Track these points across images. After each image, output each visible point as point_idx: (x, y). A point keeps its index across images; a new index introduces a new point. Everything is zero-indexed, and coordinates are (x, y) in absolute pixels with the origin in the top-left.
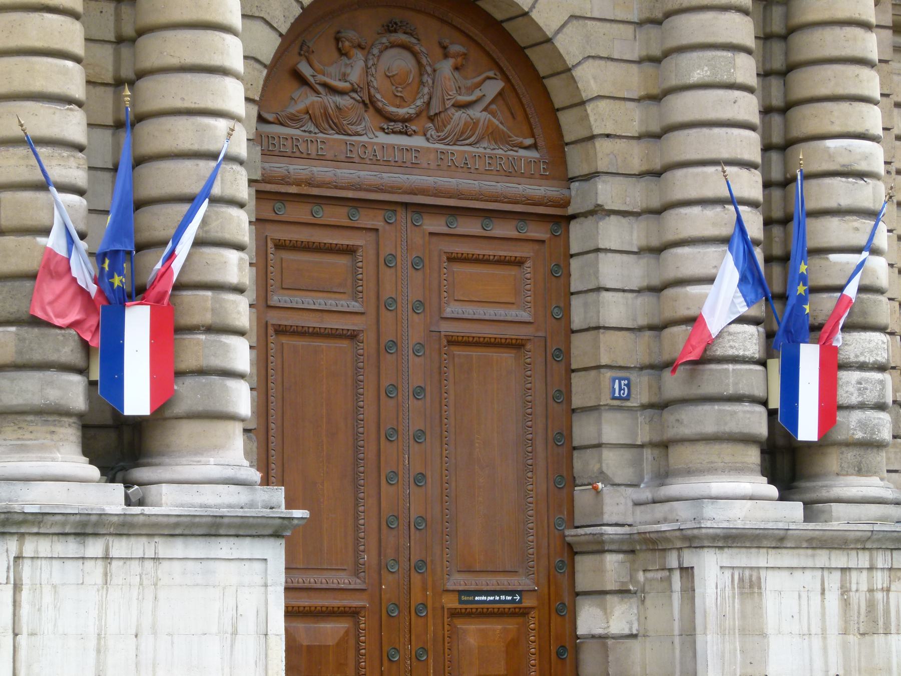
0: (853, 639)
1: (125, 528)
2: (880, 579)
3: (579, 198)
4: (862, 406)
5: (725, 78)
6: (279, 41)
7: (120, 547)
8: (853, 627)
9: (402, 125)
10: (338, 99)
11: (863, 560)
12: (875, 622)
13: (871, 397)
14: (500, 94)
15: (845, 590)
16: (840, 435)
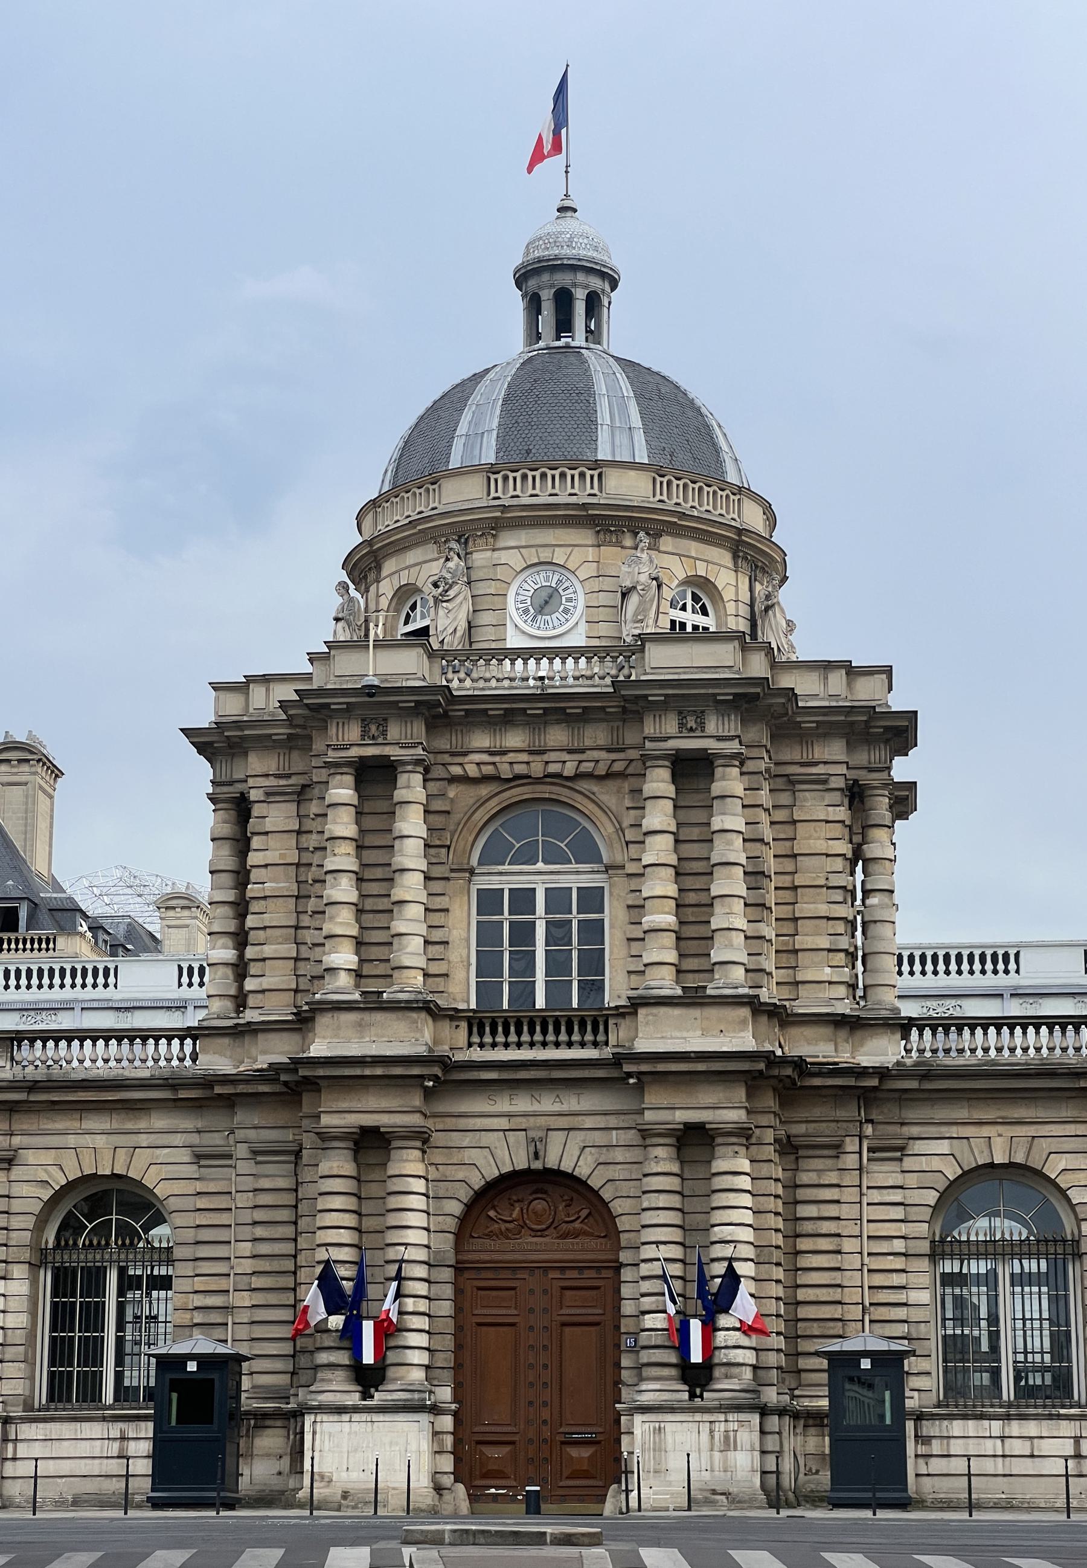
0: (717, 1455)
1: (355, 1409)
2: (732, 1426)
3: (624, 1257)
4: (726, 1347)
5: (653, 1205)
6: (463, 1206)
7: (356, 1417)
8: (716, 1448)
9: (541, 1233)
10: (508, 1225)
11: (722, 1417)
12: (729, 1445)
13: (730, 1343)
14: (589, 1214)
15: (711, 1431)
16: (716, 1361)
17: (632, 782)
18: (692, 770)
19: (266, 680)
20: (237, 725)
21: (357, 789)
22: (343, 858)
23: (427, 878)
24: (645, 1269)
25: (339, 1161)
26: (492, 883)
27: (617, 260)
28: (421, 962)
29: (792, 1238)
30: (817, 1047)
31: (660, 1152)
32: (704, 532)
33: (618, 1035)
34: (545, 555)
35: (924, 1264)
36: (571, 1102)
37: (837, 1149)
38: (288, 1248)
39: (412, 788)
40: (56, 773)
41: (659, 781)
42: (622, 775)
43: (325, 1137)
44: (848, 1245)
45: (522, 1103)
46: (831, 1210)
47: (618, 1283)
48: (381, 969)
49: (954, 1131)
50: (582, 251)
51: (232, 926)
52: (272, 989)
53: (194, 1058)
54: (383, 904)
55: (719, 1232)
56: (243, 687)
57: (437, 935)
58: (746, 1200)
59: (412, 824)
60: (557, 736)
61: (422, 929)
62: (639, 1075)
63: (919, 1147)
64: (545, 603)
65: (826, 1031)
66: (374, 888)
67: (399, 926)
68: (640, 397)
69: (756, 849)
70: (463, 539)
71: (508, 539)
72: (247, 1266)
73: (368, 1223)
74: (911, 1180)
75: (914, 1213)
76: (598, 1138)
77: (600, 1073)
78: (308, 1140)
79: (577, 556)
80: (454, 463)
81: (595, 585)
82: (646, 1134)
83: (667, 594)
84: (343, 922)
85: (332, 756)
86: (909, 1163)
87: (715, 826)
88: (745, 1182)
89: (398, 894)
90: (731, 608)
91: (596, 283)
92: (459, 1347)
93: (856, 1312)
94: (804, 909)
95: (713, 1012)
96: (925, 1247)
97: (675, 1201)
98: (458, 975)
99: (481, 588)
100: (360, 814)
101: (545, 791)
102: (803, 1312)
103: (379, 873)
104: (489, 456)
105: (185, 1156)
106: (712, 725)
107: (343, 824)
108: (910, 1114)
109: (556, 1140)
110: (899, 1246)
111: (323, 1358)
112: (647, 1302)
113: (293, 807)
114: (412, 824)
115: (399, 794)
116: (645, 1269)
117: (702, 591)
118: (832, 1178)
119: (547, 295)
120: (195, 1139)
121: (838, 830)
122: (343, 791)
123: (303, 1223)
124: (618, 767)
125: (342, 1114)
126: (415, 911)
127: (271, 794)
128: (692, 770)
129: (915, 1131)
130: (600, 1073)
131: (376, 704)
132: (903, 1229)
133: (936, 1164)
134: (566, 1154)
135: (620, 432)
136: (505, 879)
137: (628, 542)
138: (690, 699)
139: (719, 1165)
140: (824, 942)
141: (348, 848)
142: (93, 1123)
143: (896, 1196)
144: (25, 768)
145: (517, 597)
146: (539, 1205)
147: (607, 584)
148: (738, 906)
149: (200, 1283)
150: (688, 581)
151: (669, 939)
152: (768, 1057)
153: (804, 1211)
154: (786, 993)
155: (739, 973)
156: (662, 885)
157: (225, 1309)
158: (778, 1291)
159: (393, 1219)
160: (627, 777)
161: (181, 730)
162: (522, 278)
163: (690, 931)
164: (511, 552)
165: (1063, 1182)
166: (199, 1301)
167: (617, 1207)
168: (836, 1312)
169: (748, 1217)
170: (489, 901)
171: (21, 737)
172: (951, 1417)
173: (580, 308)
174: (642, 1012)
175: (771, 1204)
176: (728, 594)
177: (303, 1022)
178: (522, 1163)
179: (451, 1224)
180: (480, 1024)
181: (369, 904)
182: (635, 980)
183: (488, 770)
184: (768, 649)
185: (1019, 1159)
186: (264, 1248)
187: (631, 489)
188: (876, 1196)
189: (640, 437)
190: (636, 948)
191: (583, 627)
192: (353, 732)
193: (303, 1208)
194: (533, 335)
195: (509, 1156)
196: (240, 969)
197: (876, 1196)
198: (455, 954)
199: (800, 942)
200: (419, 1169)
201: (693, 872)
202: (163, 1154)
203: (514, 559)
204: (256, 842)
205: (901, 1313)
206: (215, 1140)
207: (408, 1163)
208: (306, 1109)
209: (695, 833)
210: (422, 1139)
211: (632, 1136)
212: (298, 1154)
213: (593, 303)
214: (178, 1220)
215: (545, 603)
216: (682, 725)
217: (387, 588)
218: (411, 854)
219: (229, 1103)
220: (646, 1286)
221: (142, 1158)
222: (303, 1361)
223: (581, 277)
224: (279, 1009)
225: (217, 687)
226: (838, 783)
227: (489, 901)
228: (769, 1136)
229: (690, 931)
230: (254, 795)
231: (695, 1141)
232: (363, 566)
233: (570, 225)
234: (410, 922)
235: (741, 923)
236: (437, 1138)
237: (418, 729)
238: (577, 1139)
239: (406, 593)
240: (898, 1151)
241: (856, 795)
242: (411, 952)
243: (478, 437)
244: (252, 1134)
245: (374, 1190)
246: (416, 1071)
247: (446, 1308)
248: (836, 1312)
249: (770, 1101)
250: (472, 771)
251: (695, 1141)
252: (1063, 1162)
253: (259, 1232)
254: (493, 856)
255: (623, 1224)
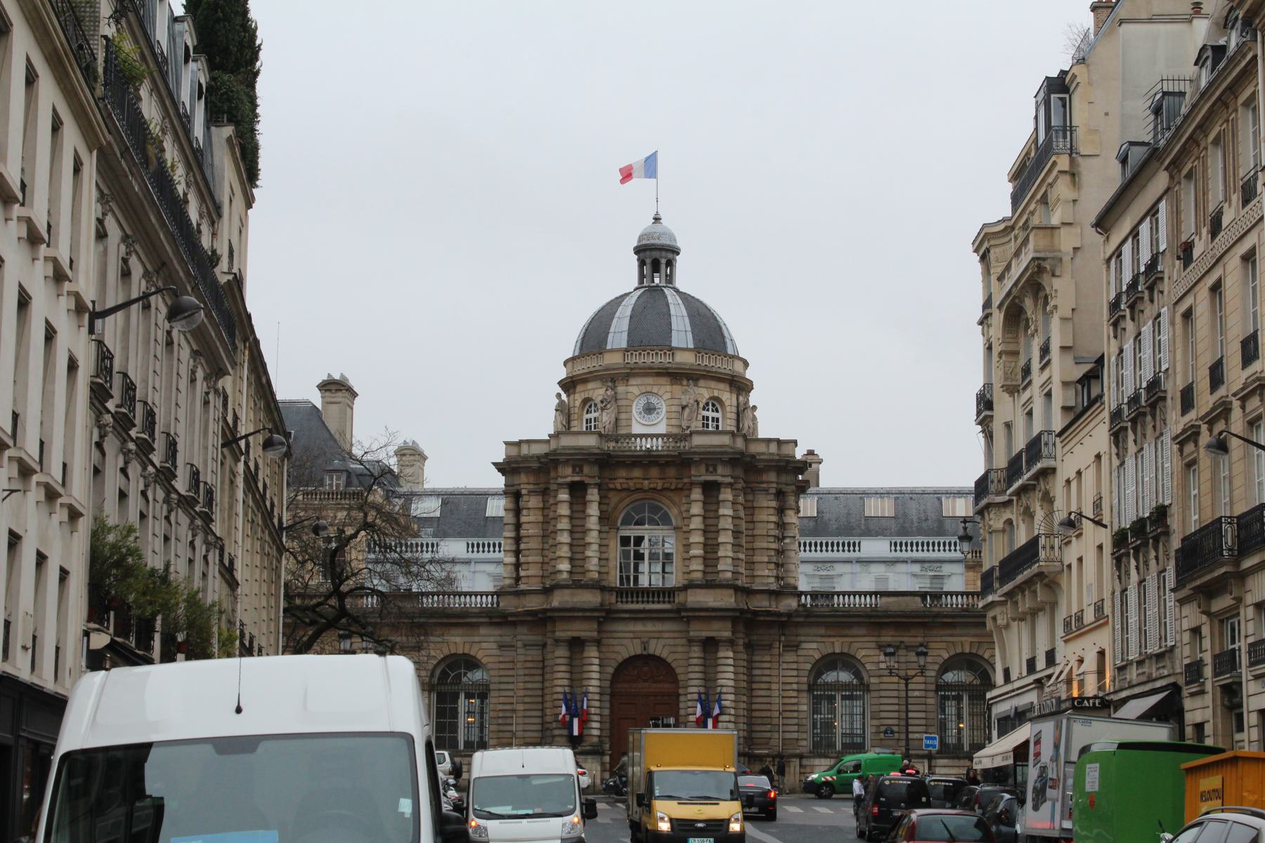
3: (681, 691)
17: (686, 492)
18: (710, 489)
19: (528, 442)
20: (517, 462)
21: (571, 494)
22: (564, 524)
23: (600, 532)
24: (689, 697)
25: (562, 652)
26: (626, 533)
27: (679, 244)
28: (597, 568)
29: (749, 686)
30: (761, 603)
31: (696, 649)
32: (718, 378)
33: (679, 598)
34: (649, 389)
35: (805, 695)
36: (659, 627)
37: (770, 646)
38: (540, 685)
39: (593, 495)
40: (354, 395)
41: (697, 494)
42: (681, 489)
43: (557, 641)
44: (774, 686)
45: (639, 627)
46: (767, 672)
47: (678, 702)
48: (580, 570)
49: (819, 639)
50: (664, 241)
51: (514, 548)
52: (532, 575)
53: (498, 604)
54: (581, 542)
55: (721, 682)
56: (519, 443)
57: (604, 556)
58: (731, 669)
59: (593, 510)
60: (654, 472)
61: (598, 554)
62: (688, 617)
63: (804, 645)
64: (649, 409)
65: (765, 596)
66: (577, 536)
67: (589, 553)
68: (690, 316)
69: (737, 522)
70: (613, 381)
71: (633, 381)
72: (521, 693)
73: (576, 676)
74: (801, 659)
75: (801, 673)
76: (671, 642)
77: (671, 615)
78: (549, 642)
79: (663, 389)
80: (609, 347)
81: (670, 402)
82: (691, 641)
83: (701, 405)
84: (564, 551)
85: (560, 480)
86: (800, 652)
87: (720, 526)
88: (731, 661)
89: (588, 539)
90: (728, 409)
91: (670, 256)
92: (611, 728)
93: (776, 714)
94: (758, 545)
95: (718, 591)
96: (805, 687)
97: (701, 669)
98: (612, 572)
99: (621, 403)
100: (571, 504)
101: (649, 495)
102: (755, 714)
103: (579, 529)
104: (624, 345)
105: (494, 646)
106: (720, 470)
107: (564, 510)
108: (802, 631)
109: (653, 642)
110: (795, 686)
111: (557, 732)
112: (690, 710)
113: (540, 498)
114: (593, 510)
115: (589, 497)
116: (689, 697)
117: (716, 403)
118: (768, 658)
119: (648, 261)
120: (499, 639)
121: (772, 511)
122: (564, 496)
123: (547, 676)
124: (680, 486)
125: (566, 631)
126: (595, 547)
127: (530, 492)
128: (710, 489)
129: (803, 638)
130: (671, 615)
131: (579, 459)
132: (796, 680)
133: (811, 652)
134: (656, 648)
135: (682, 333)
136: (632, 532)
137: (685, 382)
138: (711, 459)
139: (721, 654)
140: (766, 559)
141: (566, 520)
142: (454, 631)
143: (795, 666)
144: (340, 394)
145: (637, 407)
146: (646, 669)
147: (676, 402)
148: (729, 547)
149: (502, 700)
150: (711, 398)
151: (700, 561)
152: (742, 611)
153: (756, 672)
154: (749, 580)
155: (729, 575)
156: (697, 538)
157: (514, 711)
158: (744, 706)
159: (585, 676)
160: (684, 490)
161: (494, 464)
162: (638, 250)
163: (709, 556)
164: (633, 388)
165: (863, 661)
166: (501, 707)
167: (678, 670)
168: (768, 714)
169: (732, 676)
170: (625, 541)
171: (337, 377)
172: (814, 757)
173: (663, 267)
174: (689, 591)
175: (742, 670)
176: (727, 403)
177: (547, 591)
178: (639, 652)
179: (609, 677)
180: (621, 593)
181: (575, 542)
182: (686, 576)
183: (625, 486)
184: (744, 436)
185: (845, 651)
186: (529, 686)
187: (686, 359)
188: (785, 666)
189: (690, 335)
190: (687, 562)
191: (665, 421)
192: (569, 471)
193: (548, 670)
194: (642, 276)
195: (634, 649)
196: (517, 565)
197: (785, 666)
198: (611, 564)
199: (756, 559)
200: (597, 654)
201: (711, 532)
202: (484, 645)
203: (635, 390)
204: (525, 512)
205: (795, 714)
206: (508, 639)
207: (592, 653)
208: (549, 628)
209: (712, 514)
210: (598, 643)
211: (684, 641)
212: (544, 645)
213: (670, 263)
214: (492, 673)
215: (649, 409)
216: (707, 470)
217: (578, 398)
218: (593, 522)
219: (514, 624)
220: (690, 704)
221: (476, 647)
222: (548, 733)
223: (664, 253)
224: (535, 585)
225: (506, 443)
226: (773, 491)
227: (625, 541)
228: (741, 642)
229: (709, 556)
230: (524, 492)
231: (710, 645)
232: (568, 385)
233: (658, 228)
234: (592, 552)
235: (730, 554)
236: (605, 641)
237: (596, 470)
238: (662, 642)
239: (586, 401)
240: (796, 647)
241: (780, 494)
242: (593, 565)
243: (618, 336)
244: (524, 637)
245: (577, 662)
246: (596, 614)
247: (607, 712)
248: (768, 714)
249: (741, 627)
250: (619, 487)
251: (710, 645)
252: (863, 652)
253: (527, 679)
254: (627, 522)
255: (681, 677)
